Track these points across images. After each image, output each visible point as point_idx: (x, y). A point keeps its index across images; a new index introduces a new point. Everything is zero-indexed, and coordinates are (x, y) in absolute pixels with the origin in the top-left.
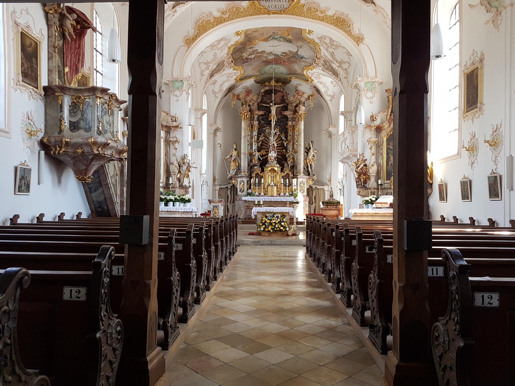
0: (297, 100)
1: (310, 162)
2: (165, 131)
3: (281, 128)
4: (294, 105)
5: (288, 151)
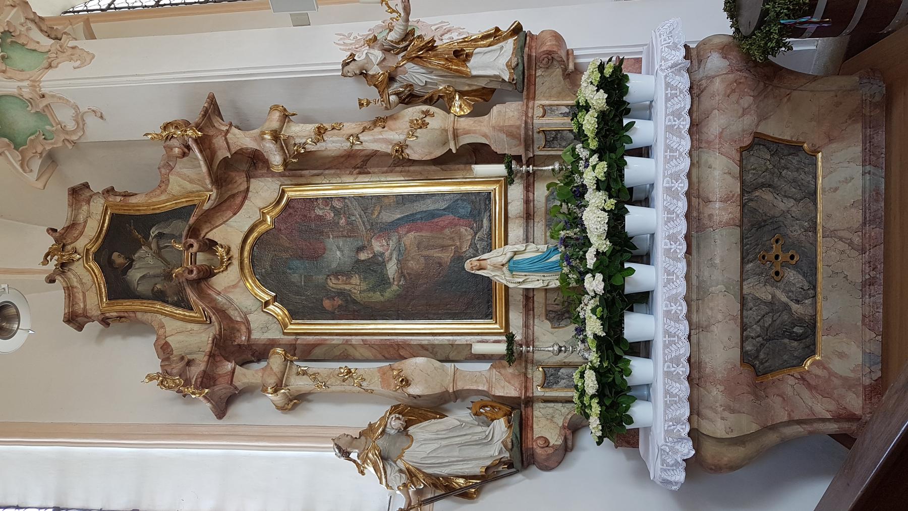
2: (249, 178)
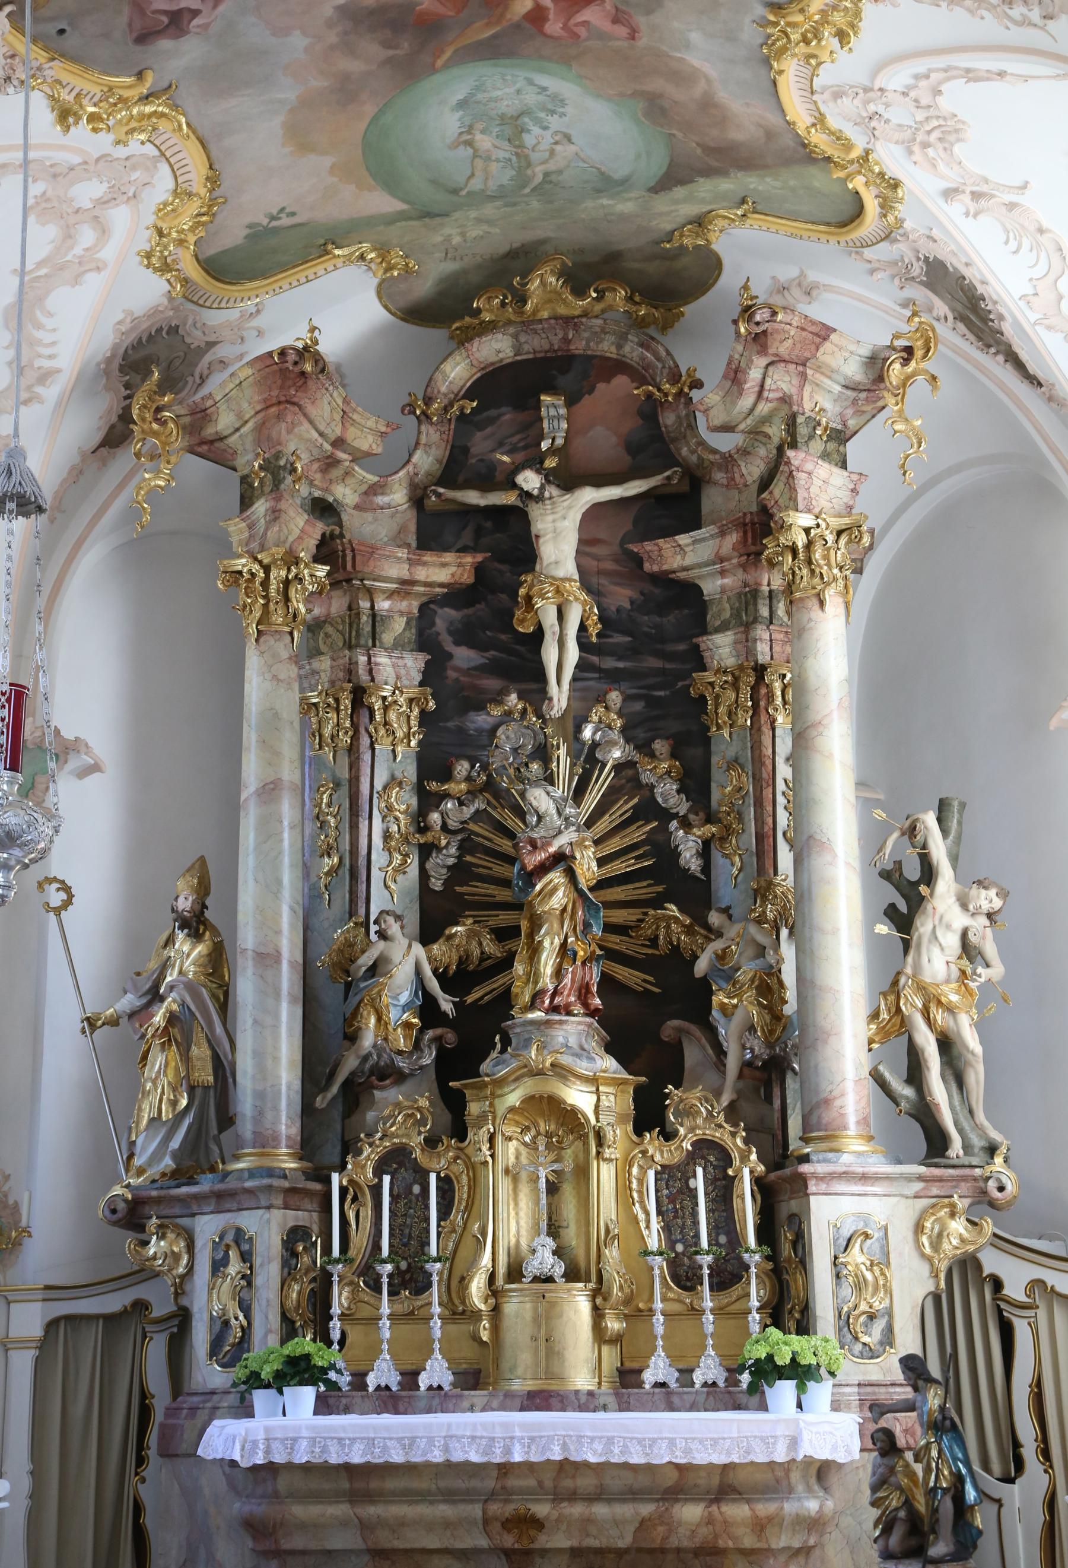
0: (767, 420)
1: (939, 1016)
3: (638, 706)
4: (753, 470)
5: (715, 918)
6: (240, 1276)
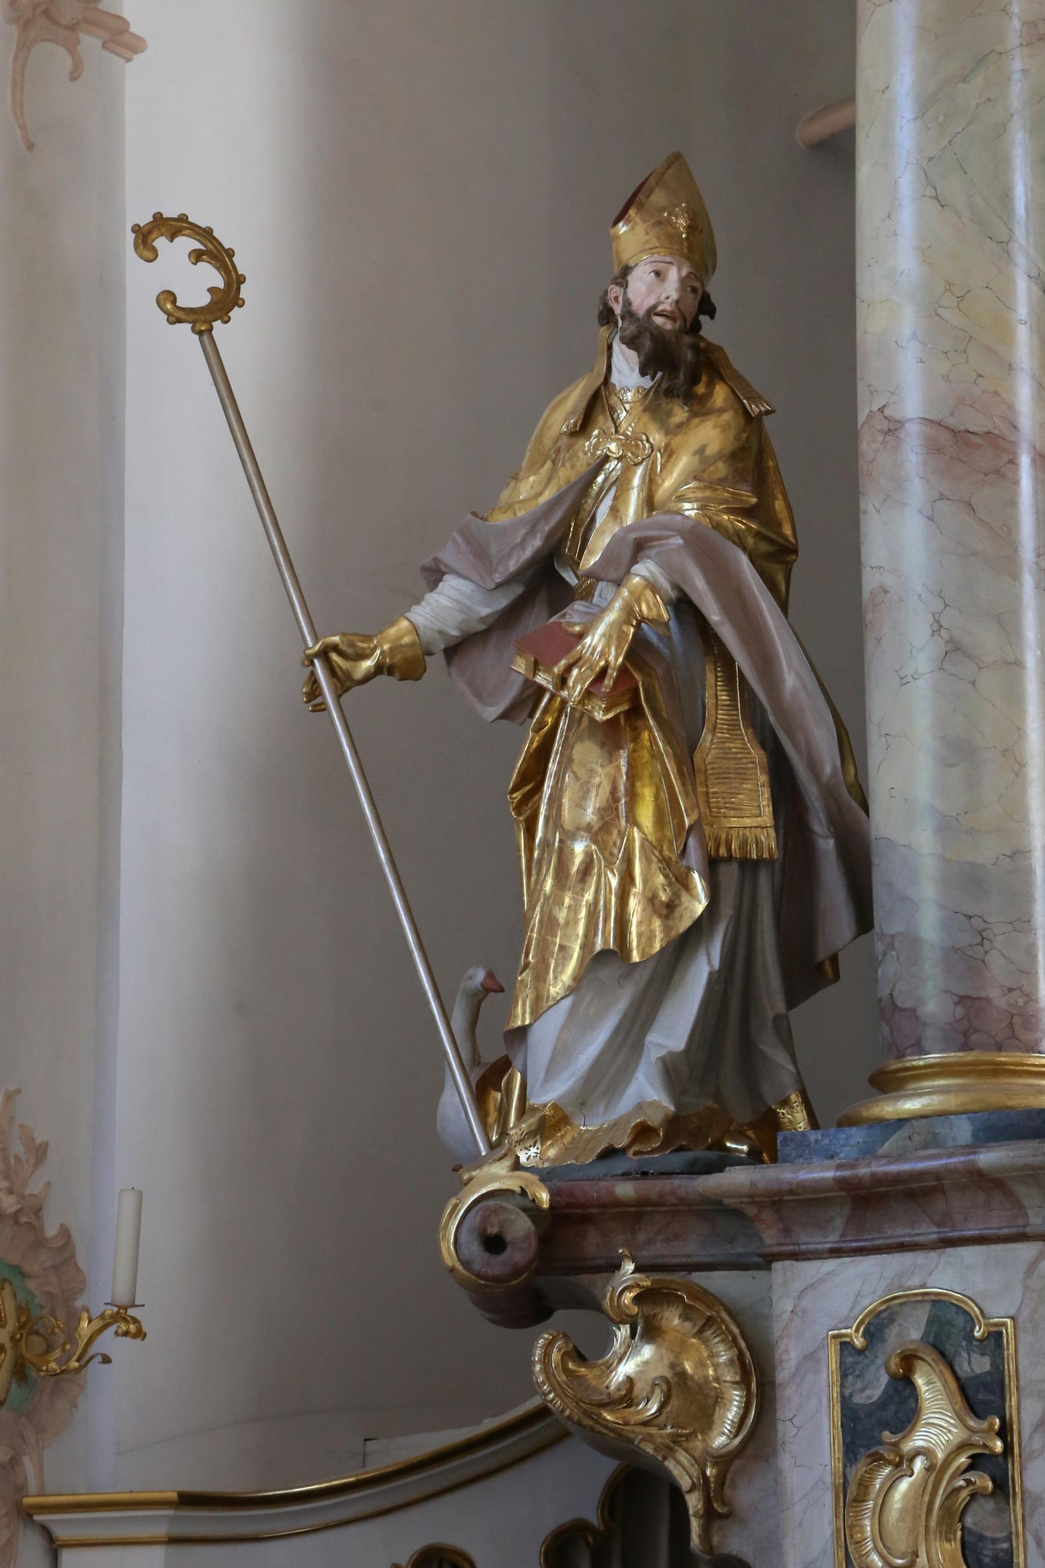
6: (963, 1460)
